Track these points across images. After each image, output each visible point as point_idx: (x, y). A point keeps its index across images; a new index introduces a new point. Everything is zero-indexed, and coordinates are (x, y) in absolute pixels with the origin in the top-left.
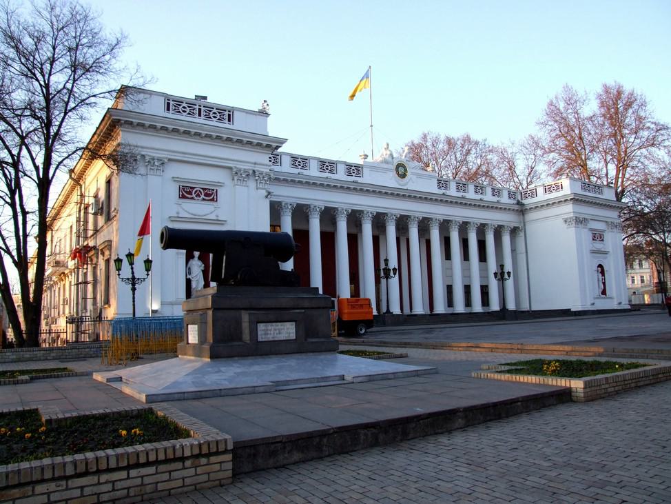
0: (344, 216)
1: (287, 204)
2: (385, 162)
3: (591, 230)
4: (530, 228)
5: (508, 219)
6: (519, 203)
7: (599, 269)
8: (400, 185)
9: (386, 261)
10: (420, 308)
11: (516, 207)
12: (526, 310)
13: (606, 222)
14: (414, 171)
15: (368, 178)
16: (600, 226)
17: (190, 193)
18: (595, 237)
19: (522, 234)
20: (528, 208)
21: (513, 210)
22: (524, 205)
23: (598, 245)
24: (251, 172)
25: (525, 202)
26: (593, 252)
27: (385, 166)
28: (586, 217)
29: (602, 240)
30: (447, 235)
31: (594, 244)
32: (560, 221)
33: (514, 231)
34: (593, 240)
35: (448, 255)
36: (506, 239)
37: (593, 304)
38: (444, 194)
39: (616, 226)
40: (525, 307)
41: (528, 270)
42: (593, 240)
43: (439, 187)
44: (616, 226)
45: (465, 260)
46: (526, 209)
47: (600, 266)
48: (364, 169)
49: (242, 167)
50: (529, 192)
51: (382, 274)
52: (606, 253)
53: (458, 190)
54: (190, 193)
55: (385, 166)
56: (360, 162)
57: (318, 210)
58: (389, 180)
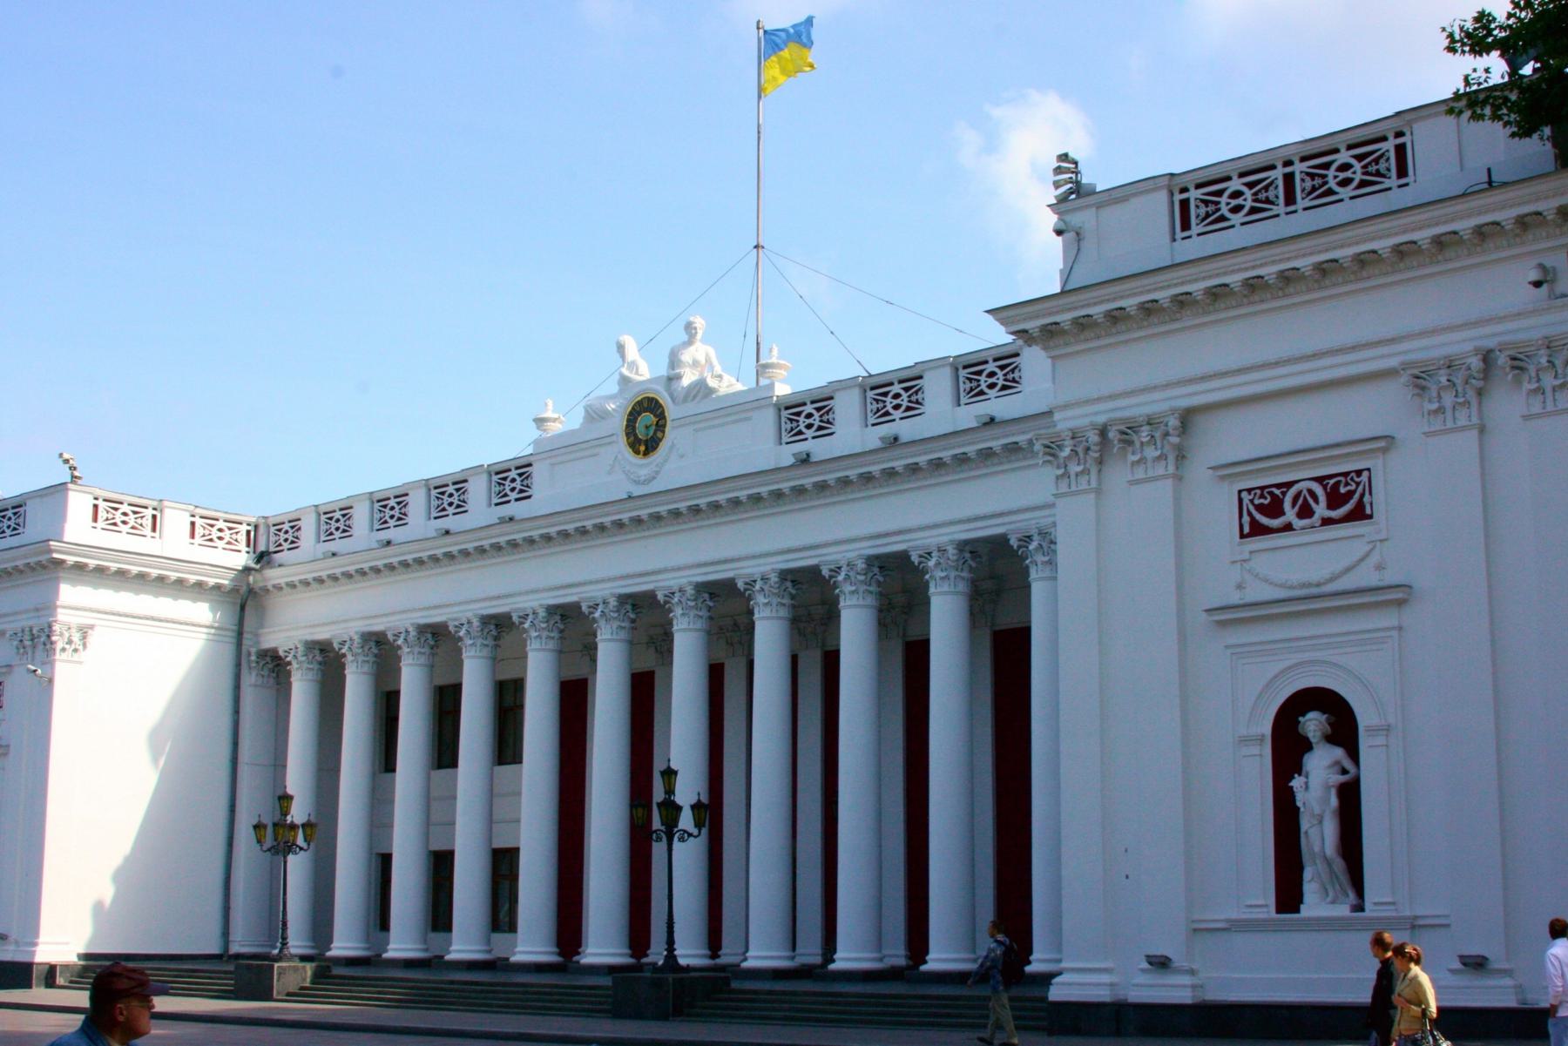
3: (1226, 471)
9: (669, 774)
10: (762, 949)
14: (691, 408)
18: (1275, 509)
23: (1310, 556)
26: (1229, 616)
29: (1360, 514)
30: (391, 688)
31: (1262, 564)
35: (386, 757)
37: (1161, 963)
38: (805, 460)
42: (1257, 530)
51: (657, 824)
58: (614, 476)
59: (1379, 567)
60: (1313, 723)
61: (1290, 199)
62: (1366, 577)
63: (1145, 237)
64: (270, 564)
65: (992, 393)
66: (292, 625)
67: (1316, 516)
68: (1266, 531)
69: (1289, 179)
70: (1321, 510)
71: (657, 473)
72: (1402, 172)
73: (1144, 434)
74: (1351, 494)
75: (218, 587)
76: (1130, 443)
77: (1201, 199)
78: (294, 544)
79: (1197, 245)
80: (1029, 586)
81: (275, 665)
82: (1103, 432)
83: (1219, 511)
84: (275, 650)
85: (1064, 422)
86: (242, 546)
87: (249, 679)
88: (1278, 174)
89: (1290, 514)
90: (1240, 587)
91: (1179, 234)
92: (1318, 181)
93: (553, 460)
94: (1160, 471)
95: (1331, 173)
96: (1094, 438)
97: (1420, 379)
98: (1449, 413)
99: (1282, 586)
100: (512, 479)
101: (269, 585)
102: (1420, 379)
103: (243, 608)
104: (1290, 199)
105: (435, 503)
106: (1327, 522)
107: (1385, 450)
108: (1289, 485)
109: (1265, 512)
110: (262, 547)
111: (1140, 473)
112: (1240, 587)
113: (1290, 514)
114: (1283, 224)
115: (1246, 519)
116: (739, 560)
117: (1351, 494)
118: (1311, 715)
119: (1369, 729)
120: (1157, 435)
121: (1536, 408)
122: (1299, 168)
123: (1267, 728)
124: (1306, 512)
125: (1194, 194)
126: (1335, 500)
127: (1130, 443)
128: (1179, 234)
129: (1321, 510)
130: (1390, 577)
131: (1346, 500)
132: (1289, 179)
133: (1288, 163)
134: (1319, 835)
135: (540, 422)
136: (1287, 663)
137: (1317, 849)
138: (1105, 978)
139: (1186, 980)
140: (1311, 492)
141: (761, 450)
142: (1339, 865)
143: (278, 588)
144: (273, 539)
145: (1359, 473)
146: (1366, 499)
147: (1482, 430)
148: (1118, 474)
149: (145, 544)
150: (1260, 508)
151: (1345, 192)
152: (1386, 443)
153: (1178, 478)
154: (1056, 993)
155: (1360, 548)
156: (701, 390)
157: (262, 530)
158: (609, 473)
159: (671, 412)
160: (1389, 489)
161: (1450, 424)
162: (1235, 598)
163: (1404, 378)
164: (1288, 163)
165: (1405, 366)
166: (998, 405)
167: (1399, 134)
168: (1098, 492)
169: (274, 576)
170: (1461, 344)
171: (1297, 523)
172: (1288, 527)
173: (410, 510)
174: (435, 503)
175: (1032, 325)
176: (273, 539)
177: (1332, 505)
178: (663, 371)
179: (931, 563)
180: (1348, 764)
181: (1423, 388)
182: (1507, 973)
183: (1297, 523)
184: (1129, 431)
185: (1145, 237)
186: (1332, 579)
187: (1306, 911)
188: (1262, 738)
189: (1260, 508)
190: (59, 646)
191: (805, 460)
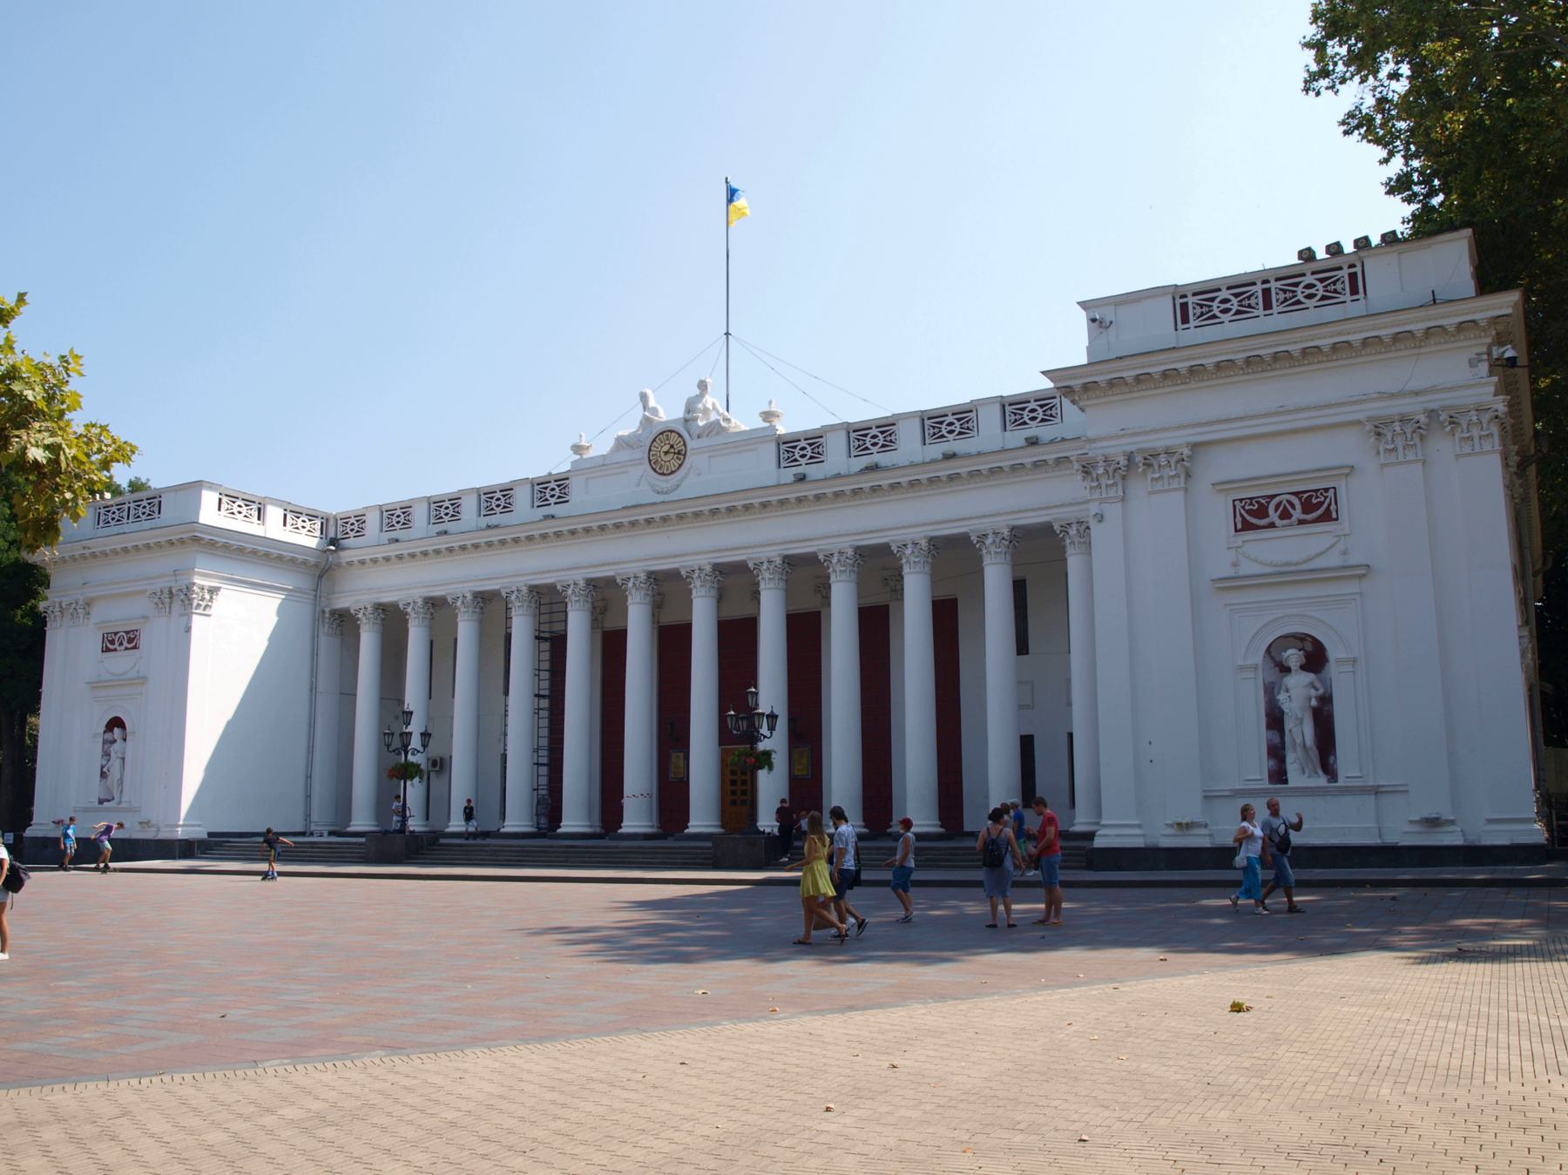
3: (1221, 486)
13: (1358, 423)
14: (704, 442)
15: (582, 499)
17: (112, 642)
18: (1262, 512)
24: (166, 594)
26: (1229, 584)
27: (625, 456)
29: (1327, 517)
39: (1453, 422)
42: (1247, 526)
44: (1453, 422)
45: (1019, 653)
49: (158, 585)
54: (112, 642)
55: (625, 456)
58: (638, 486)
59: (1344, 553)
60: (1293, 657)
61: (1268, 305)
62: (1333, 560)
63: (1160, 327)
64: (340, 548)
65: (951, 437)
66: (361, 591)
67: (1294, 518)
68: (1256, 527)
69: (1267, 292)
70: (1297, 514)
72: (1354, 291)
73: (1163, 459)
74: (1320, 504)
75: (305, 563)
76: (1150, 465)
77: (1195, 303)
78: (360, 533)
79: (1195, 333)
80: (982, 570)
81: (344, 622)
82: (1130, 457)
83: (1219, 515)
84: (347, 610)
85: (1097, 451)
86: (318, 533)
87: (325, 629)
88: (1258, 288)
89: (1273, 516)
90: (1235, 565)
91: (1180, 326)
92: (1289, 295)
94: (1175, 484)
95: (1299, 289)
96: (1123, 462)
98: (1400, 450)
99: (1270, 564)
100: (551, 490)
101: (344, 561)
102: (1379, 428)
103: (320, 577)
104: (1268, 305)
105: (484, 505)
106: (1301, 522)
107: (1347, 475)
108: (1272, 497)
109: (1253, 515)
110: (332, 534)
111: (1159, 486)
112: (1235, 565)
113: (1273, 516)
114: (1263, 322)
115: (1239, 518)
116: (687, 555)
117: (1320, 504)
118: (1290, 651)
119: (1338, 661)
120: (1173, 461)
121: (1467, 449)
122: (1273, 285)
123: (1258, 657)
124: (1285, 515)
125: (1191, 300)
126: (1308, 507)
127: (1150, 465)
128: (1180, 326)
129: (1297, 514)
130: (1354, 559)
131: (1316, 507)
132: (1267, 292)
133: (1265, 282)
134: (1301, 731)
135: (577, 449)
136: (1270, 618)
137: (1299, 741)
138: (1137, 831)
139: (1203, 831)
140: (1289, 502)
141: (764, 470)
142: (1314, 753)
143: (350, 564)
144: (340, 529)
145: (1327, 490)
146: (1333, 507)
147: (1424, 462)
148: (1139, 487)
149: (252, 528)
150: (1249, 512)
151: (1308, 303)
153: (1186, 490)
154: (1098, 843)
155: (1327, 541)
156: (715, 428)
157: (332, 522)
160: (1350, 500)
161: (1401, 458)
162: (1230, 572)
163: (1369, 427)
164: (1265, 282)
165: (1369, 419)
166: (954, 445)
167: (1351, 266)
168: (1123, 499)
169: (346, 556)
170: (1414, 407)
171: (1278, 522)
172: (1272, 525)
173: (463, 509)
175: (1076, 383)
176: (340, 529)
177: (1305, 511)
178: (679, 413)
179: (908, 552)
180: (1318, 685)
181: (1379, 434)
182: (1452, 822)
183: (1278, 522)
184: (1150, 459)
185: (1160, 327)
186: (1310, 559)
187: (1291, 784)
188: (1256, 668)
189: (1249, 512)
190: (195, 603)
191: (801, 478)
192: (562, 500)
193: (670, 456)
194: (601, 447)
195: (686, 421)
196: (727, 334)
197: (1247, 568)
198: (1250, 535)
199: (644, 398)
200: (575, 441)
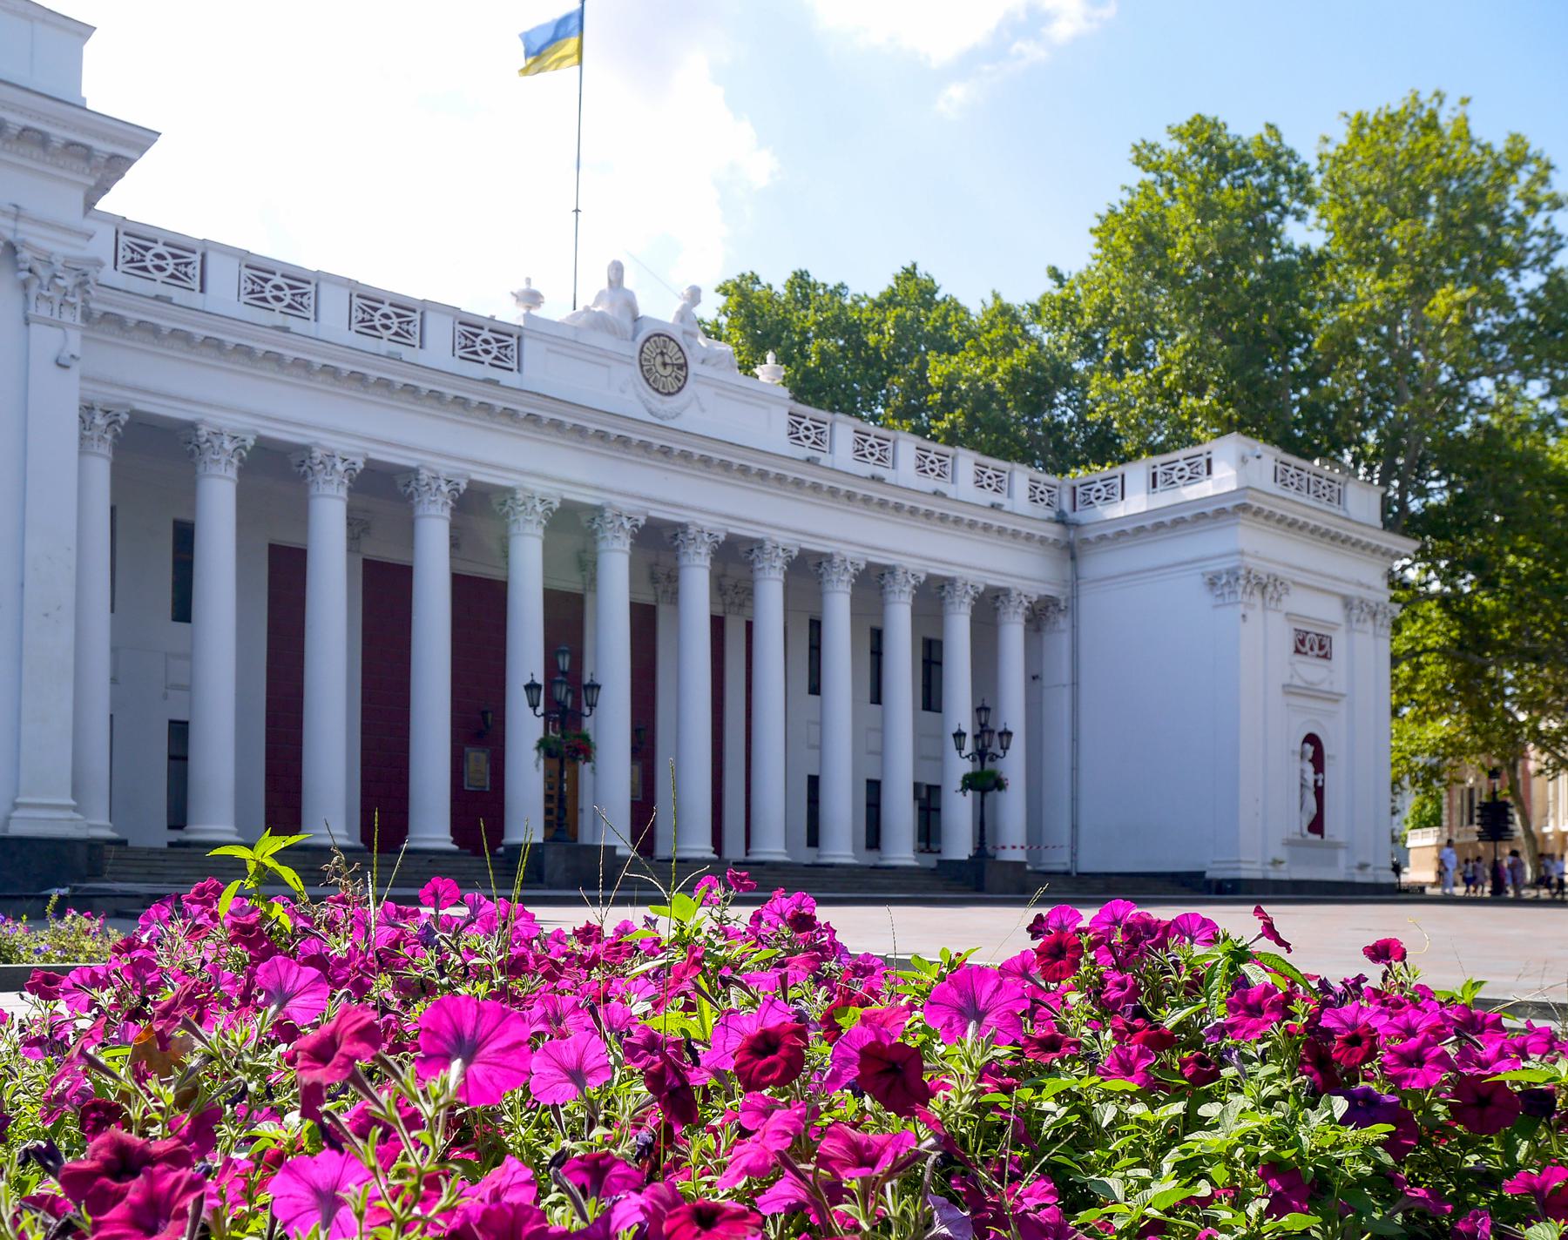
0: (441, 499)
1: (218, 434)
2: (599, 322)
4: (1092, 602)
5: (1023, 571)
6: (1061, 519)
7: (1309, 749)
8: (651, 413)
11: (1052, 532)
12: (1061, 868)
16: (1326, 611)
18: (1302, 642)
19: (1064, 623)
20: (1091, 536)
21: (1043, 540)
22: (1077, 525)
25: (1084, 515)
26: (1289, 690)
28: (1280, 571)
29: (1325, 657)
32: (1193, 583)
33: (1039, 616)
34: (1297, 651)
36: (1013, 634)
40: (1058, 860)
41: (1075, 740)
42: (1297, 651)
43: (795, 437)
46: (1086, 541)
47: (1312, 739)
48: (526, 343)
50: (1099, 485)
52: (1333, 698)
53: (861, 455)
56: (510, 314)
57: (340, 467)
70: (1316, 647)
71: (678, 414)
93: (554, 348)
97: (1347, 603)
126: (1321, 647)
130: (1336, 690)
135: (532, 298)
152: (1335, 626)
158: (623, 392)
159: (694, 367)
174: (415, 329)
192: (499, 363)
193: (669, 369)
194: (555, 310)
195: (685, 332)
196: (577, 211)
197: (1297, 682)
198: (1299, 657)
199: (617, 270)
200: (524, 286)
